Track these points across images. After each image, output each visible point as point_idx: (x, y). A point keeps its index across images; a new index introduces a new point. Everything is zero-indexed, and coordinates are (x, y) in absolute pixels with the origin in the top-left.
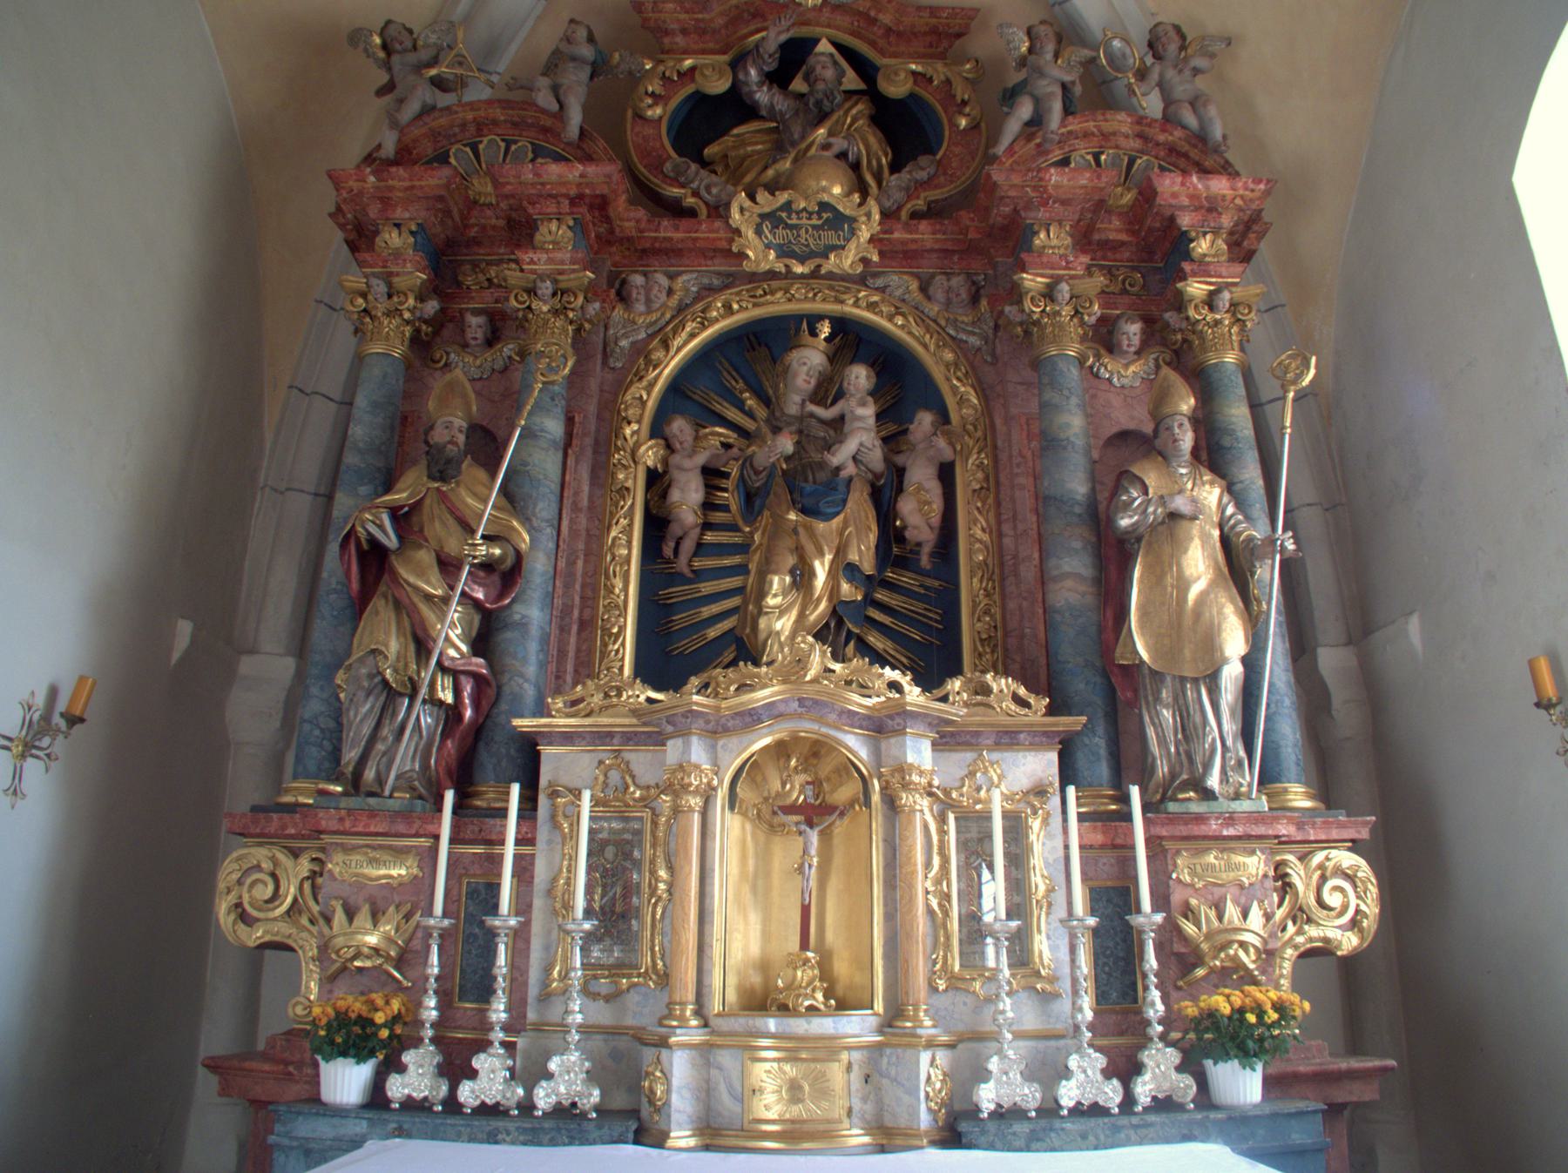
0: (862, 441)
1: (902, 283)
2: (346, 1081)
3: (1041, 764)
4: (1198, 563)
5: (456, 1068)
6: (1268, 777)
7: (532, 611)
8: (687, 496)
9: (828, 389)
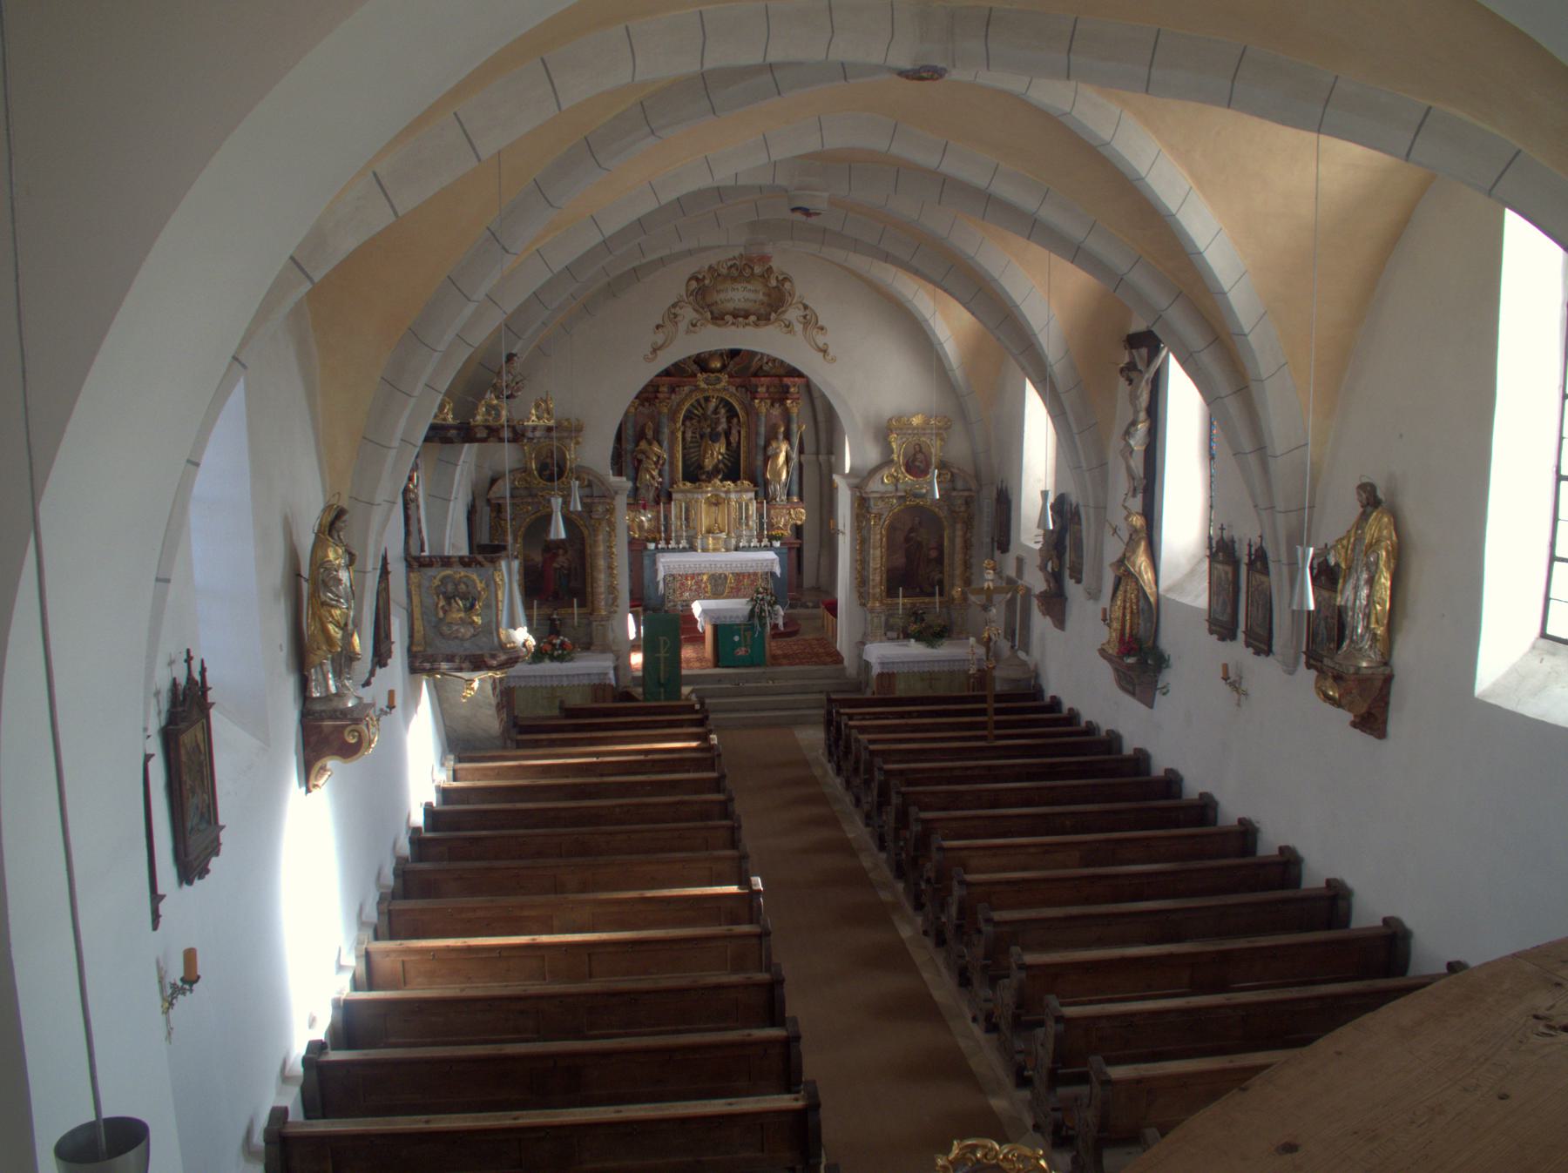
0: (723, 426)
1: (733, 389)
2: (652, 546)
3: (752, 495)
4: (782, 458)
5: (668, 543)
6: (789, 494)
8: (689, 435)
9: (716, 411)
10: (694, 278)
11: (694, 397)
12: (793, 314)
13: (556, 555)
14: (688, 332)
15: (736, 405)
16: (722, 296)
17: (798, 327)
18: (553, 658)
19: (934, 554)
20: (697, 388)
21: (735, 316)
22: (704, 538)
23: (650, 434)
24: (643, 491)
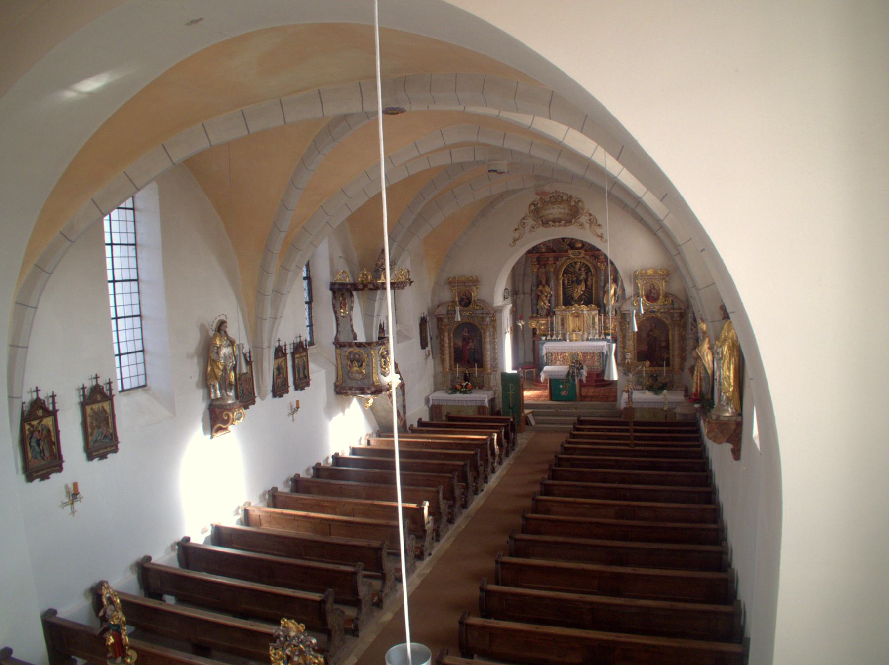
0: (583, 277)
1: (588, 257)
2: (544, 338)
3: (597, 312)
4: (612, 292)
5: (552, 336)
7: (553, 298)
8: (566, 282)
9: (580, 269)
10: (533, 204)
11: (569, 262)
12: (584, 219)
13: (468, 342)
14: (530, 231)
15: (590, 265)
16: (547, 212)
17: (587, 225)
18: (461, 392)
19: (663, 344)
20: (569, 258)
21: (554, 222)
22: (571, 334)
23: (544, 282)
24: (540, 311)
